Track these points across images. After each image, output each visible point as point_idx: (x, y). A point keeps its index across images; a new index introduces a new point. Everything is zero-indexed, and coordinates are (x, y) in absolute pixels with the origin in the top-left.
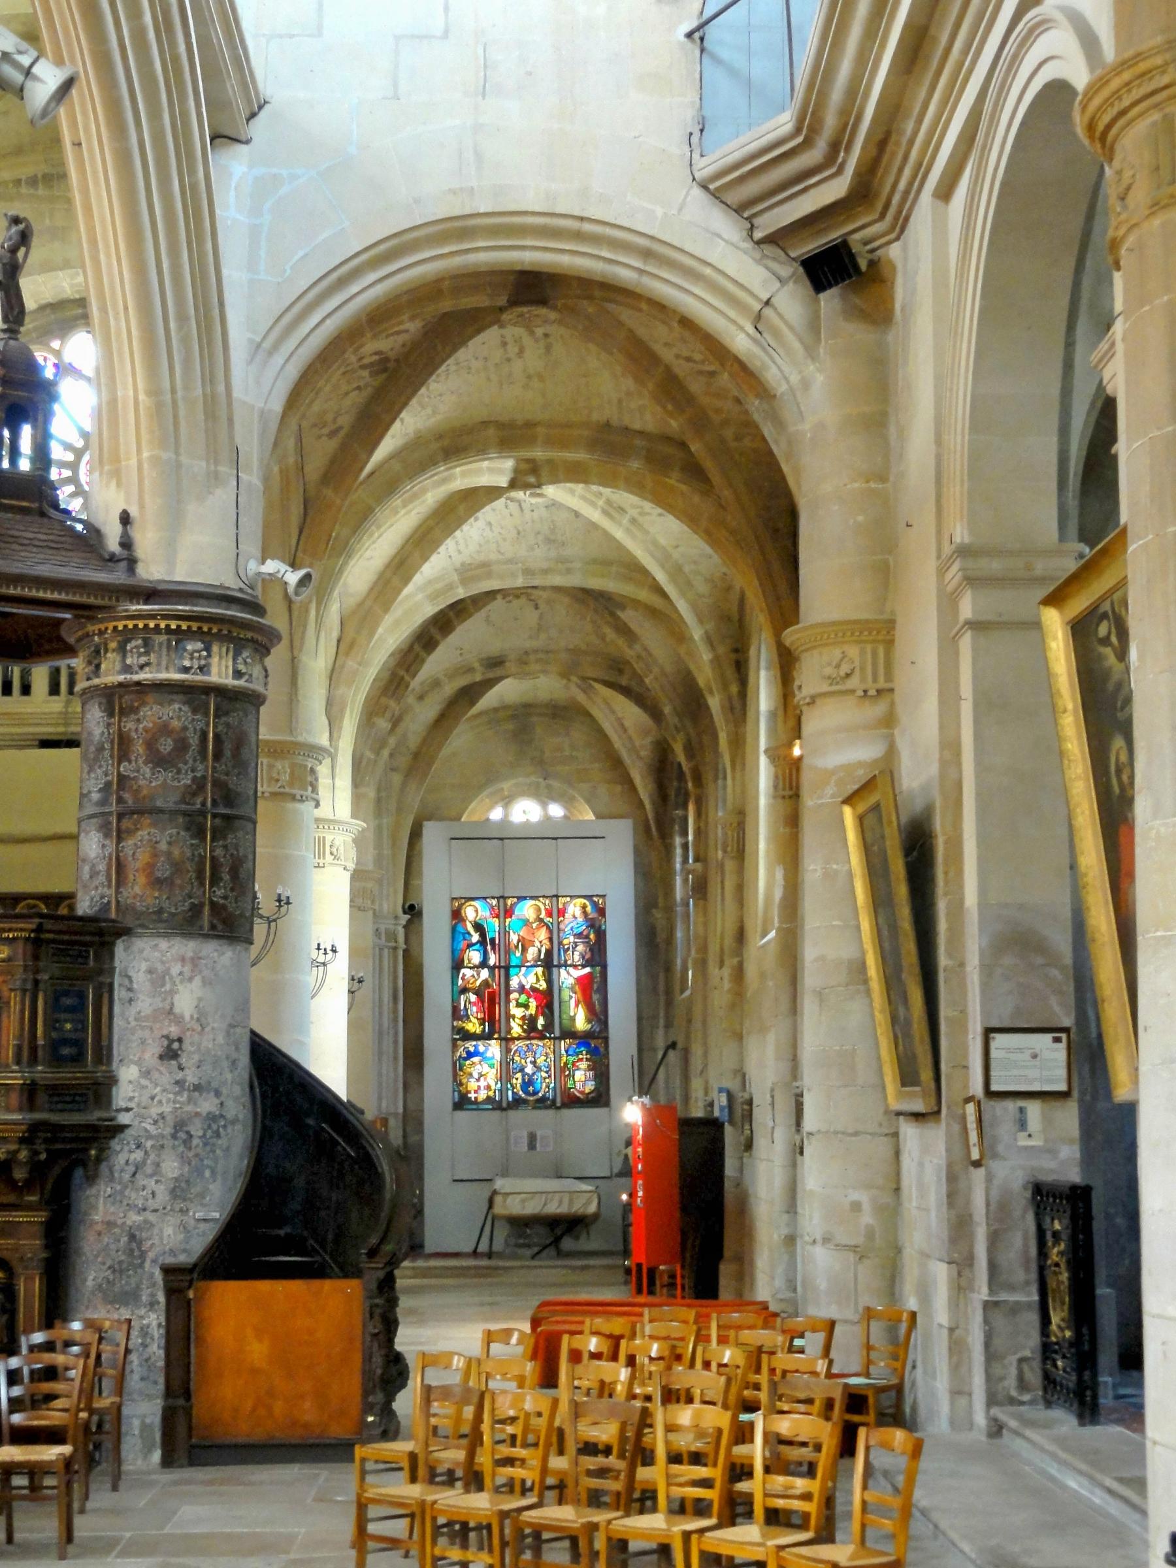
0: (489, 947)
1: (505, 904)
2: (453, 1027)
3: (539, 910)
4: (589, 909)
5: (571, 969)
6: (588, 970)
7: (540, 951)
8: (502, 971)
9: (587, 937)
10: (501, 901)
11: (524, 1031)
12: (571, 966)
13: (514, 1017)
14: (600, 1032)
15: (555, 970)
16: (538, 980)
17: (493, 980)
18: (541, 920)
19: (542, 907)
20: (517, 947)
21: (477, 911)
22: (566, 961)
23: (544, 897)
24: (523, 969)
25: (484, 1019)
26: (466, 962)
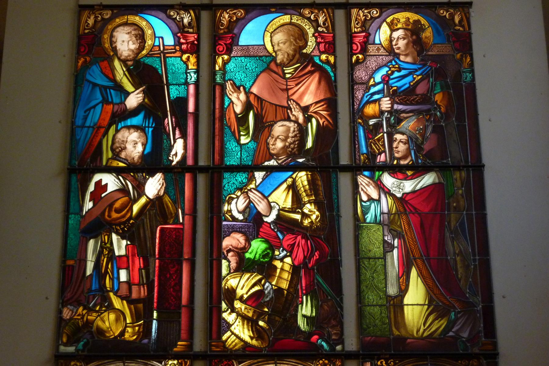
0: (169, 122)
1: (215, 24)
2: (60, 321)
3: (302, 35)
4: (428, 34)
5: (388, 180)
6: (428, 179)
7: (302, 132)
8: (202, 179)
9: (426, 99)
10: (205, 15)
11: (258, 333)
12: (385, 168)
13: (231, 295)
14: (473, 339)
15: (344, 180)
16: (298, 202)
17: (178, 201)
18: (308, 59)
19: (310, 31)
20: (242, 120)
21: (141, 37)
22: (372, 156)
23: (312, 6)
24: (259, 175)
25: (147, 302)
26: (107, 154)
